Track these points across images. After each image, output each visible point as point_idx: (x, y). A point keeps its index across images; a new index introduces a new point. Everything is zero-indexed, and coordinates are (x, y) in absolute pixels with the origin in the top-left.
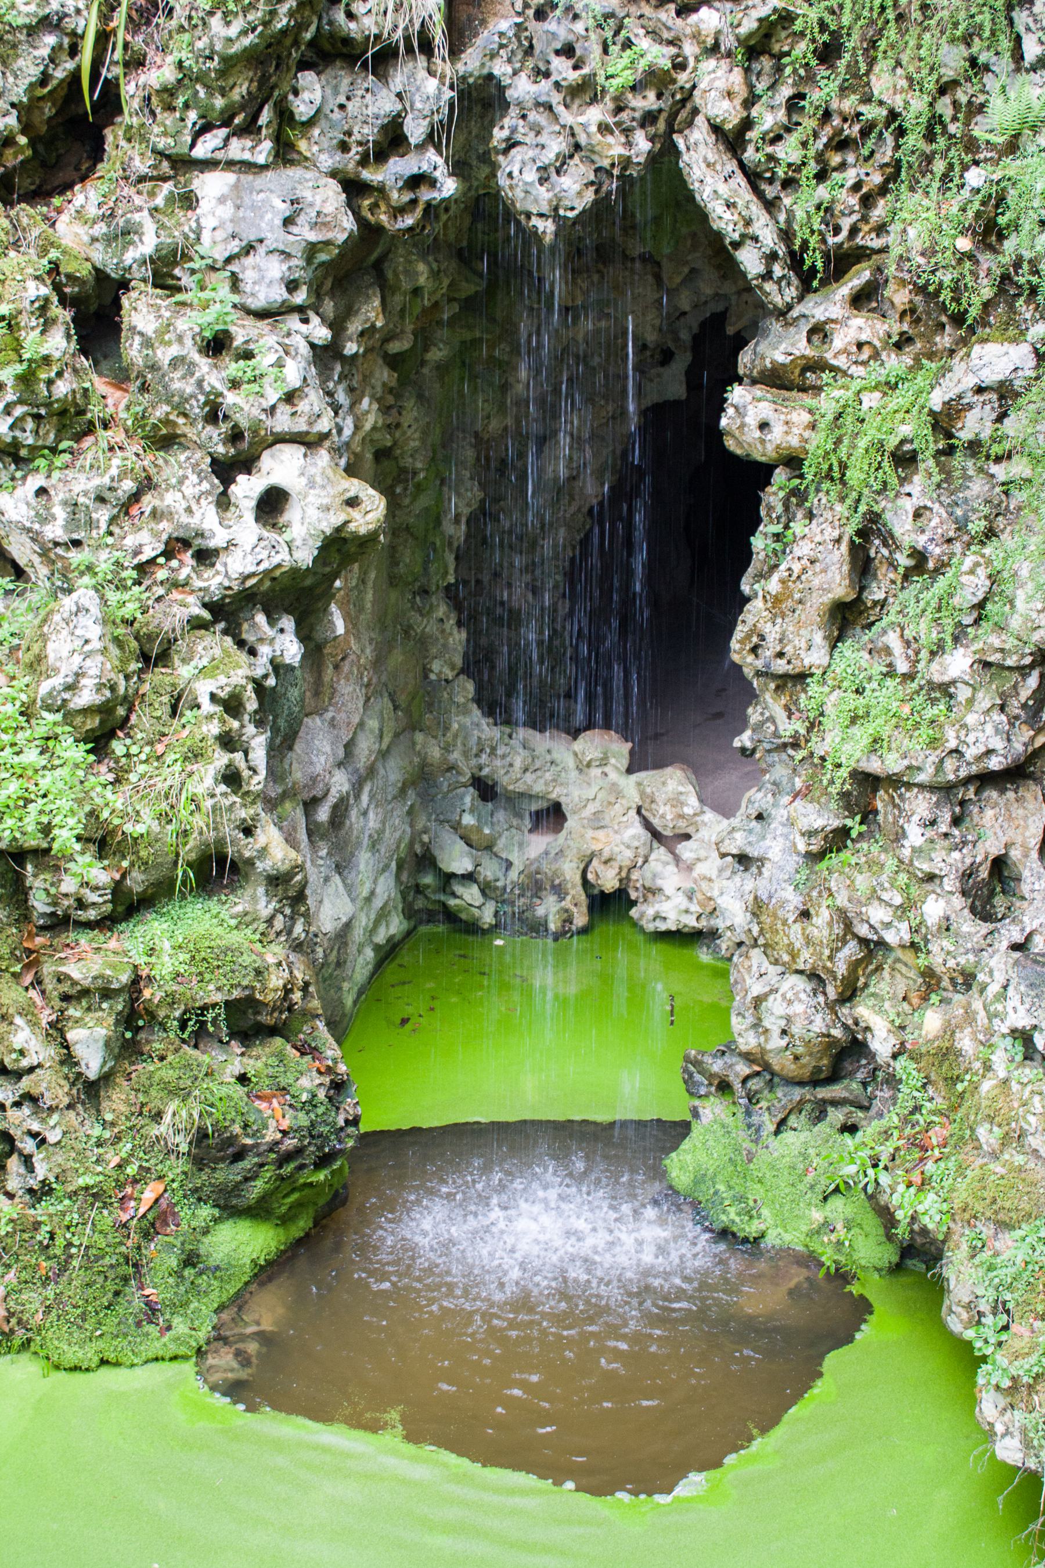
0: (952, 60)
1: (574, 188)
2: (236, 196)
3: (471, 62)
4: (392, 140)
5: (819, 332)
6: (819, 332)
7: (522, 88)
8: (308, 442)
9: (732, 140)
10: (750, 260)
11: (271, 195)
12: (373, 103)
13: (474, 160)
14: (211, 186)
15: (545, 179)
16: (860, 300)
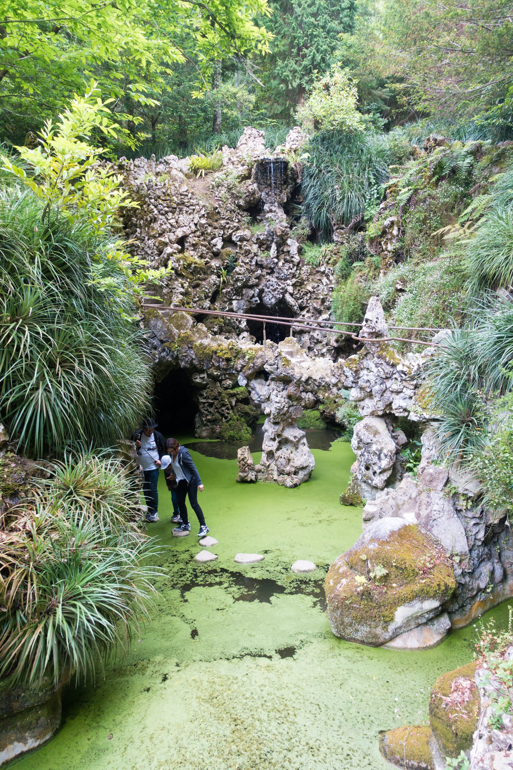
0: (316, 285)
1: (273, 301)
2: (238, 303)
3: (260, 287)
4: (253, 296)
5: (304, 316)
6: (304, 316)
7: (266, 290)
8: (247, 331)
9: (292, 295)
10: (295, 308)
11: (242, 302)
12: (251, 292)
13: (261, 299)
14: (234, 303)
15: (270, 300)
16: (308, 312)
